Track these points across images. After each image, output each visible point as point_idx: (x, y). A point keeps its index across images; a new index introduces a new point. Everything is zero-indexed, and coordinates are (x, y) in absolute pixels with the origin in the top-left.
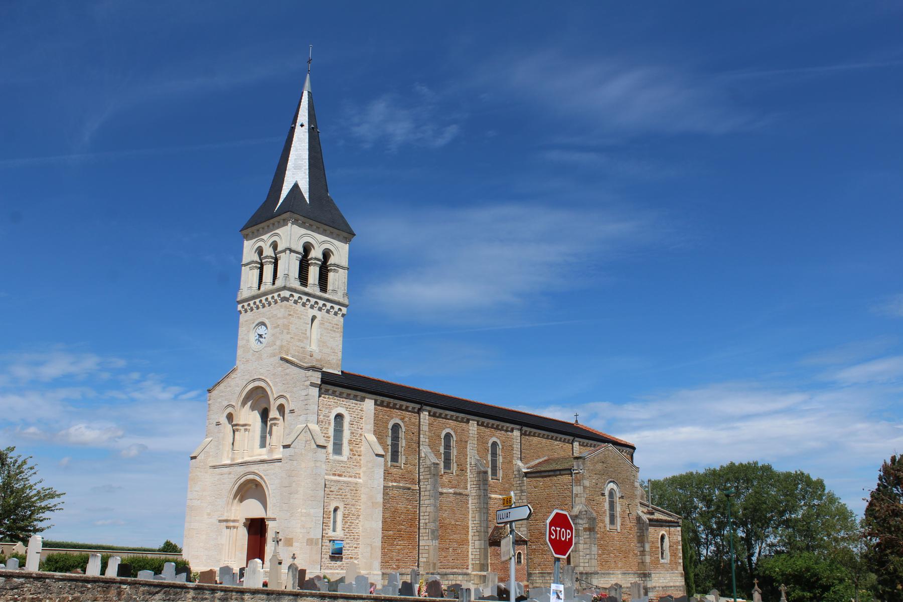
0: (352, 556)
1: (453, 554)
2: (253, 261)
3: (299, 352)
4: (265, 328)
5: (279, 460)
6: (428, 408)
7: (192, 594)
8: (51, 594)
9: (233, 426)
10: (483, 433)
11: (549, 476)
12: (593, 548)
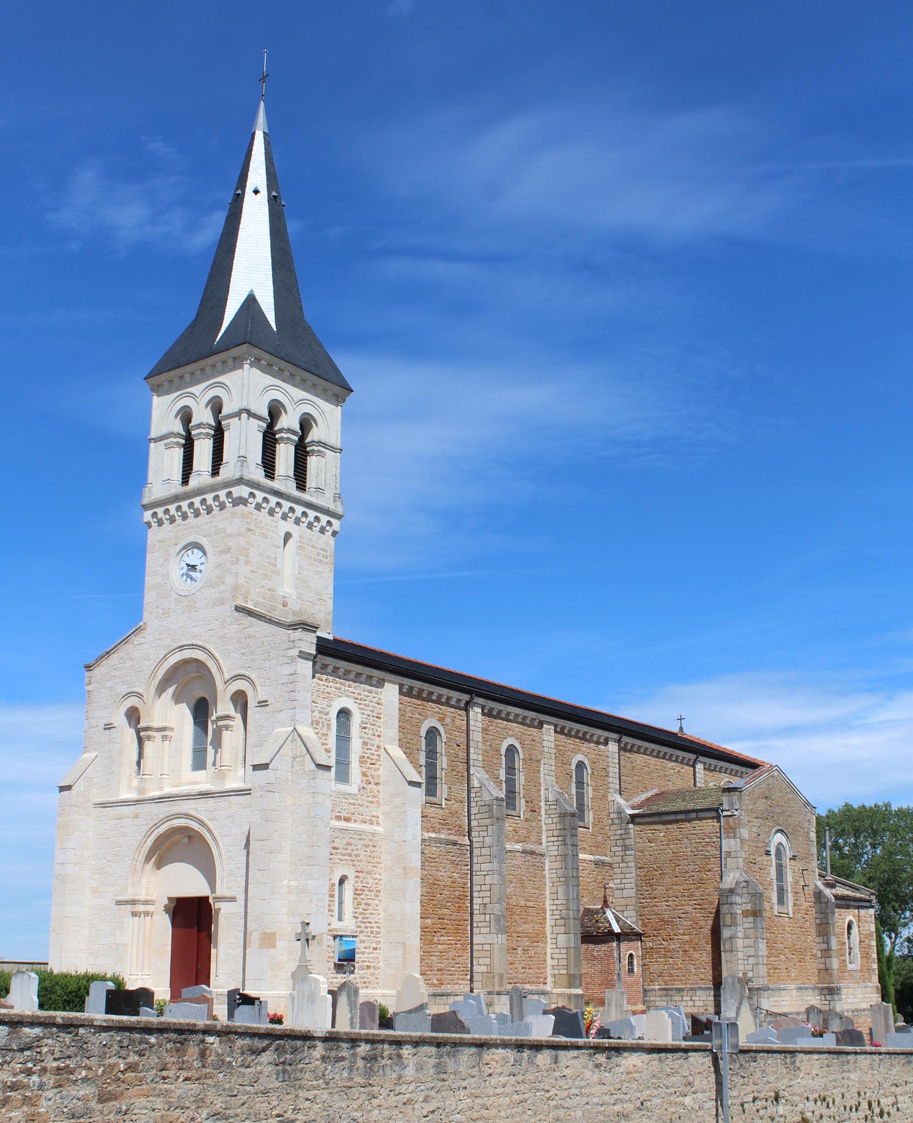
0: (369, 964)
1: (523, 958)
2: (173, 433)
3: (264, 598)
4: (200, 554)
5: (245, 792)
6: (480, 701)
7: (320, 1050)
8: (88, 1058)
9: (138, 731)
10: (563, 746)
11: (677, 821)
12: (761, 945)
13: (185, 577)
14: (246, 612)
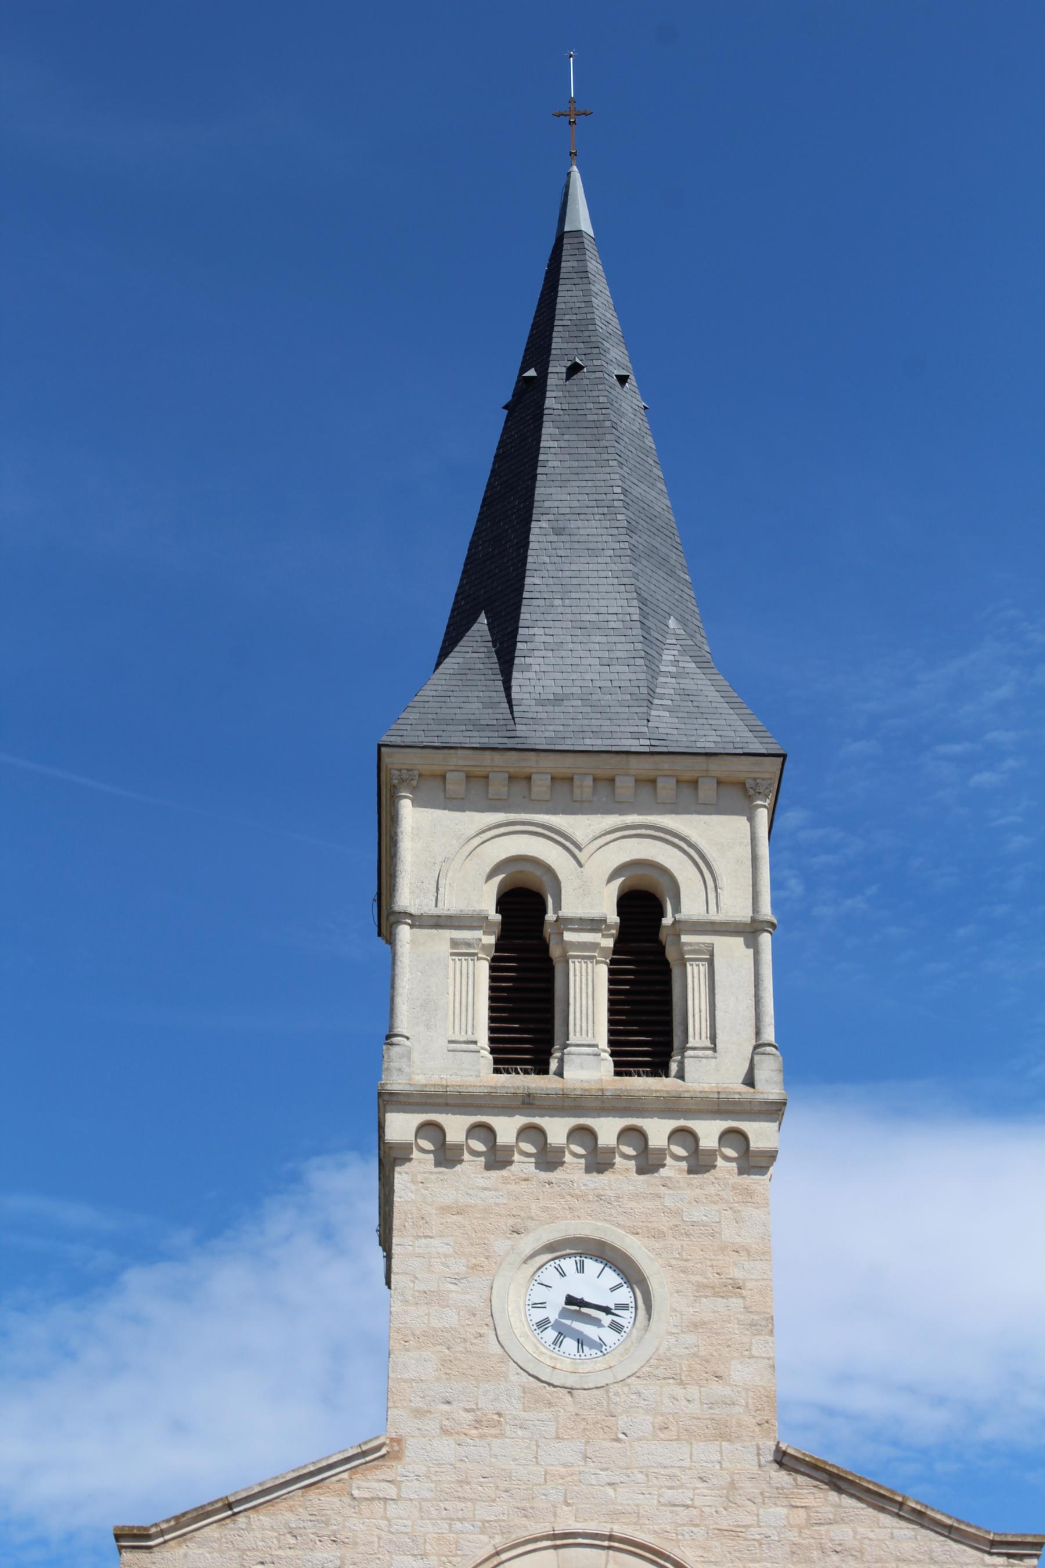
13: (551, 1334)
14: (825, 1477)
